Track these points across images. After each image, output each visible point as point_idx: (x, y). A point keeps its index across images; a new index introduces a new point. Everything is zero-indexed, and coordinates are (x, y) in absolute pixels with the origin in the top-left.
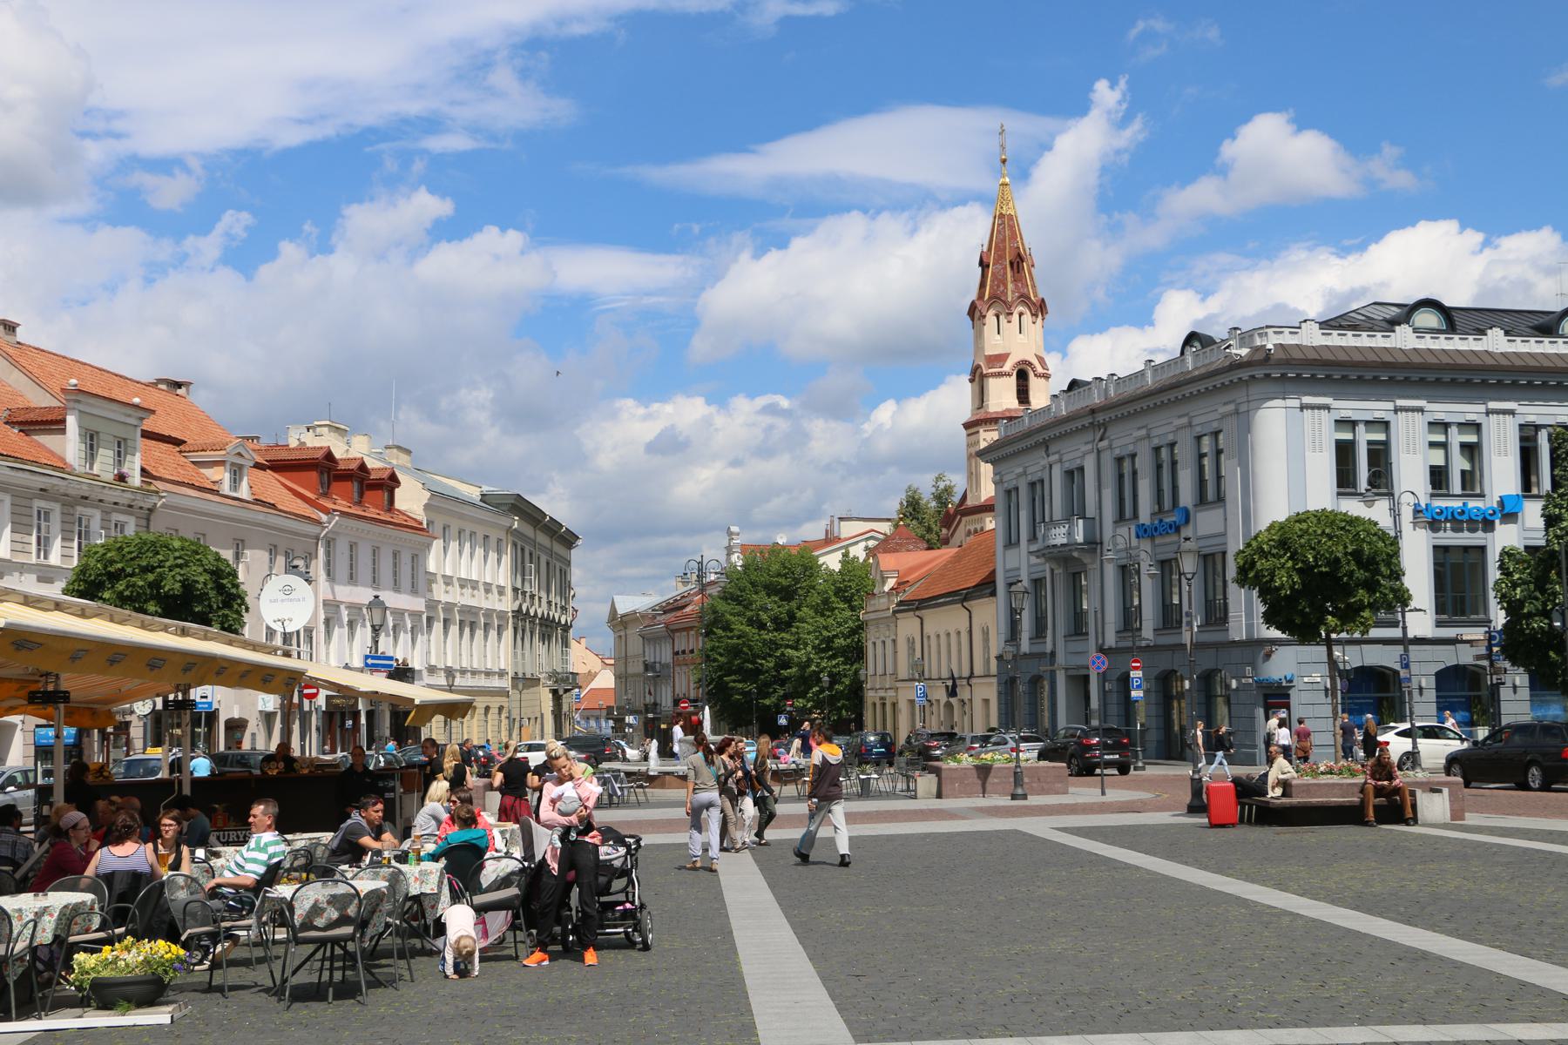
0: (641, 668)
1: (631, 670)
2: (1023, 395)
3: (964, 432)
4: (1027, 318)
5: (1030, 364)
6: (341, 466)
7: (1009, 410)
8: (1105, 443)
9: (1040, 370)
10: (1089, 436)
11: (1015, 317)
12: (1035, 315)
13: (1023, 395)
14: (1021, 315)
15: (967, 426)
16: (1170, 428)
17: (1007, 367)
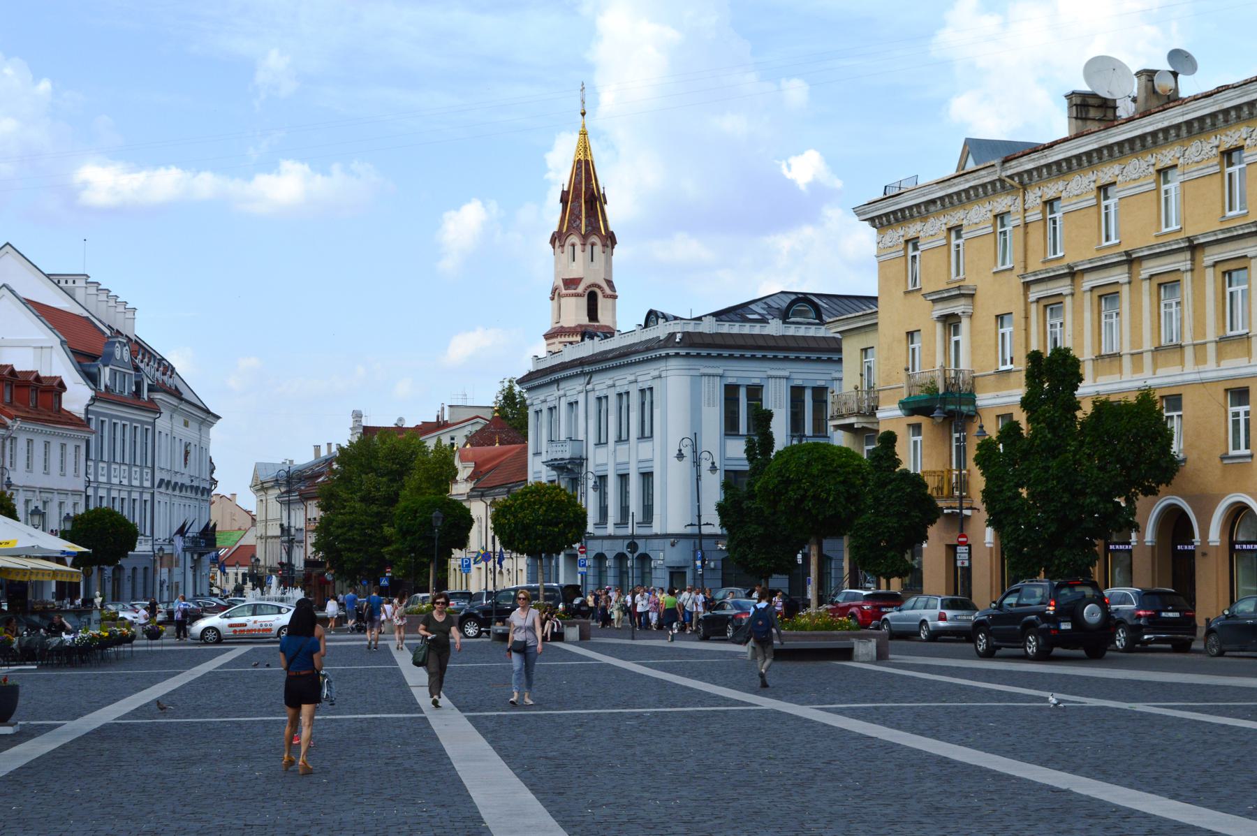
0: (278, 532)
1: (269, 534)
2: (592, 313)
3: (544, 342)
4: (598, 249)
5: (599, 287)
6: (21, 378)
7: (580, 326)
8: (589, 387)
9: (608, 291)
10: (583, 380)
11: (588, 248)
12: (605, 245)
13: (592, 313)
14: (593, 245)
15: (548, 336)
16: (649, 377)
17: (580, 289)
